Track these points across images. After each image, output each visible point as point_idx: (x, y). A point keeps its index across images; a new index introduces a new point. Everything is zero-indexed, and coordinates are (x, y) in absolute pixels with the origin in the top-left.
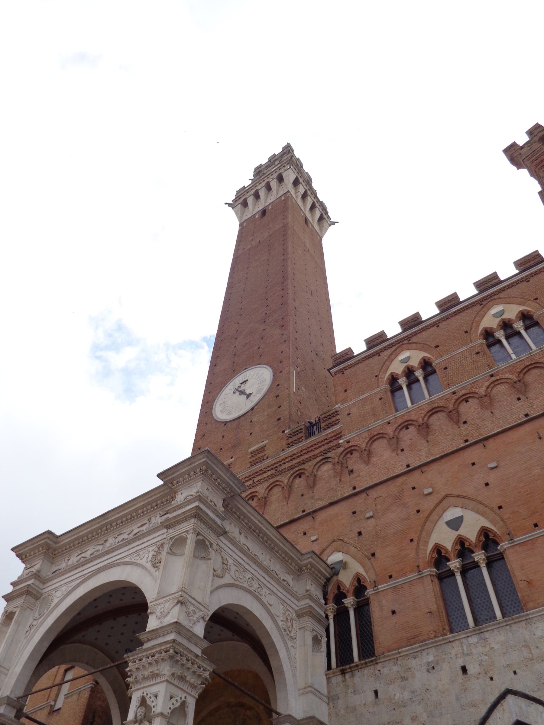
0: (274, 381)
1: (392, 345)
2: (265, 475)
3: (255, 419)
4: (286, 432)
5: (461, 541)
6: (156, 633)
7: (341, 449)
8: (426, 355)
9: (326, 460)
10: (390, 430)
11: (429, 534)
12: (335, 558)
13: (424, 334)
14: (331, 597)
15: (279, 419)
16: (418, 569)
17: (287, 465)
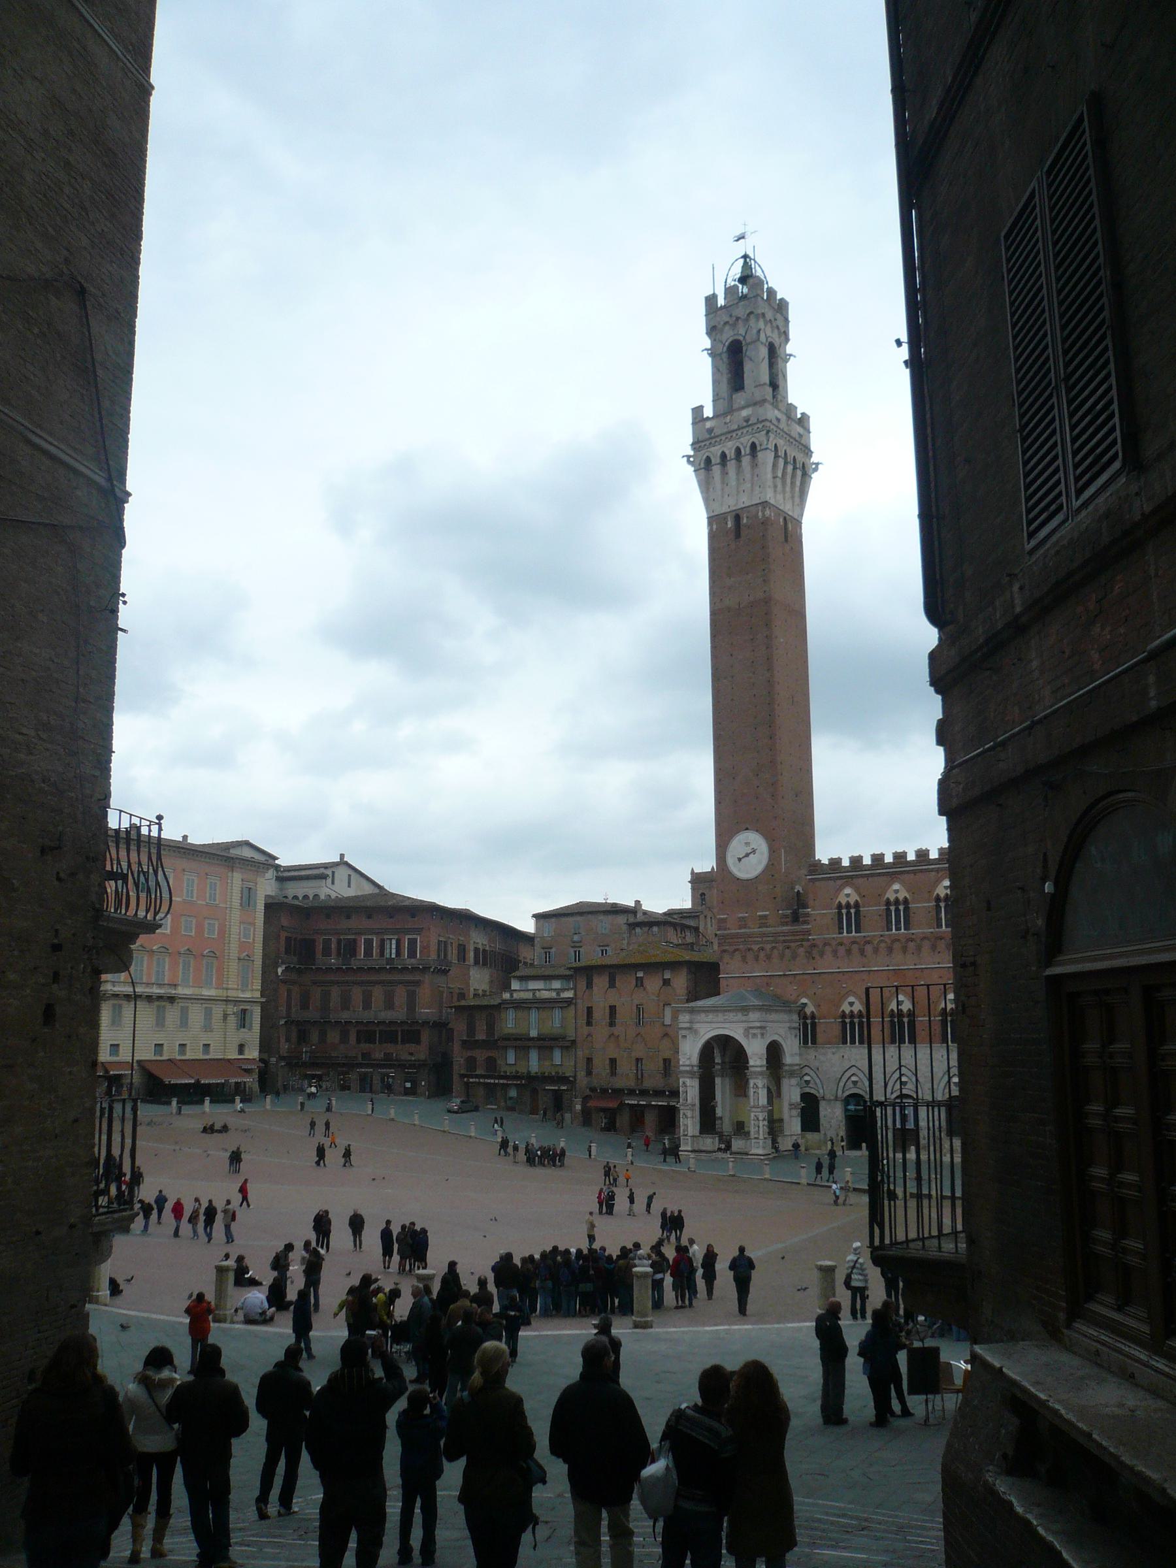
0: (770, 860)
1: (841, 878)
2: (768, 939)
3: (759, 888)
4: (780, 912)
5: (852, 1012)
6: (753, 1066)
7: (809, 943)
8: (858, 899)
9: (802, 946)
10: (834, 943)
11: (841, 1006)
12: (804, 1000)
13: (860, 881)
14: (802, 1017)
15: (775, 898)
16: (835, 1019)
17: (783, 938)
